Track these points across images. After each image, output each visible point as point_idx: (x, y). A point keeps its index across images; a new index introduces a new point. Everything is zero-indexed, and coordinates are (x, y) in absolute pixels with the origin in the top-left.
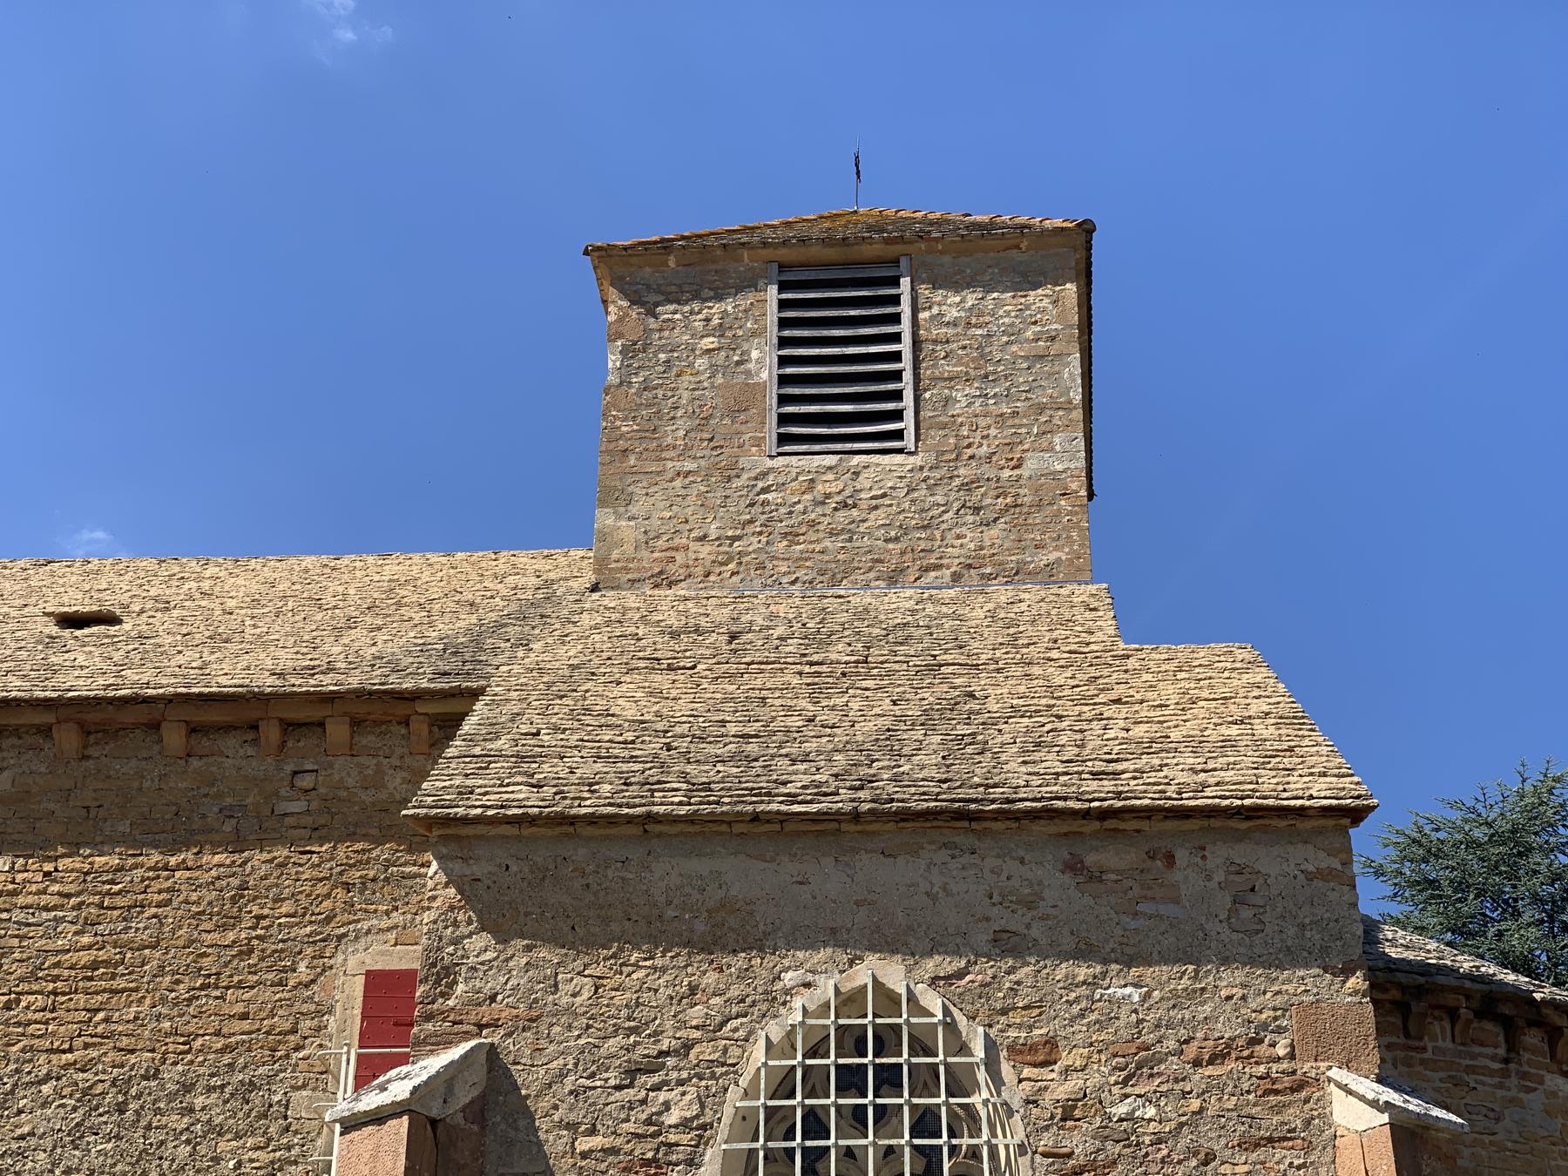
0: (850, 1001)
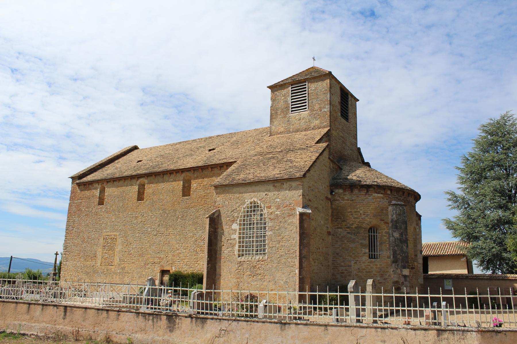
0: (251, 203)
